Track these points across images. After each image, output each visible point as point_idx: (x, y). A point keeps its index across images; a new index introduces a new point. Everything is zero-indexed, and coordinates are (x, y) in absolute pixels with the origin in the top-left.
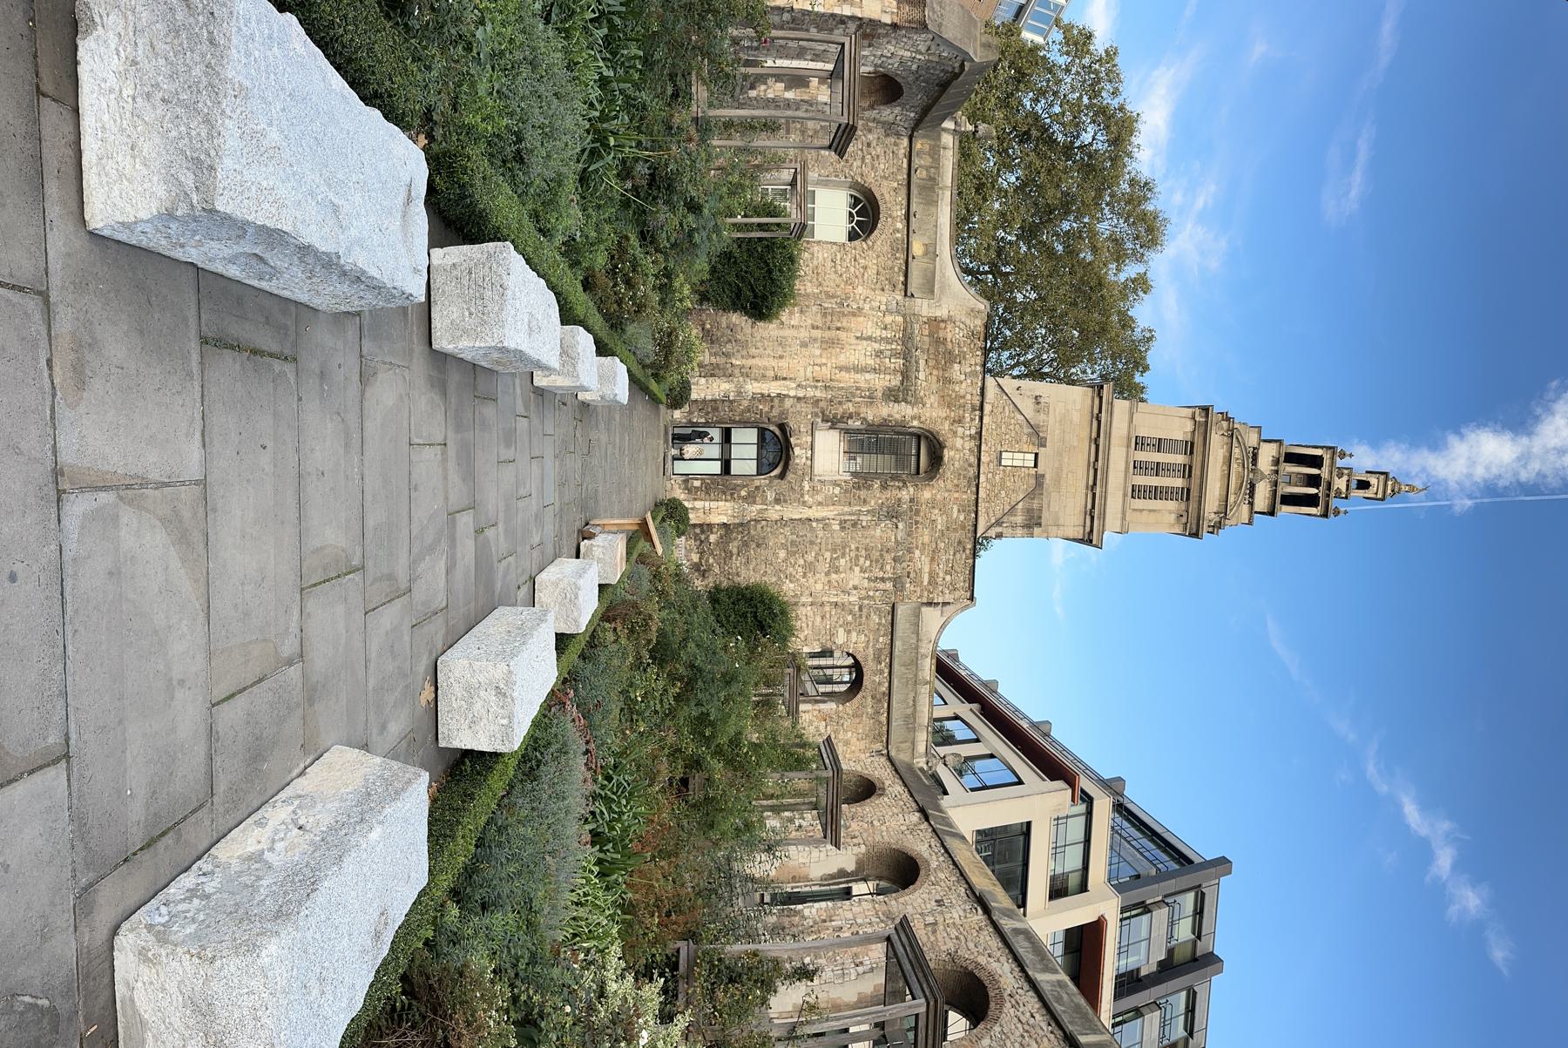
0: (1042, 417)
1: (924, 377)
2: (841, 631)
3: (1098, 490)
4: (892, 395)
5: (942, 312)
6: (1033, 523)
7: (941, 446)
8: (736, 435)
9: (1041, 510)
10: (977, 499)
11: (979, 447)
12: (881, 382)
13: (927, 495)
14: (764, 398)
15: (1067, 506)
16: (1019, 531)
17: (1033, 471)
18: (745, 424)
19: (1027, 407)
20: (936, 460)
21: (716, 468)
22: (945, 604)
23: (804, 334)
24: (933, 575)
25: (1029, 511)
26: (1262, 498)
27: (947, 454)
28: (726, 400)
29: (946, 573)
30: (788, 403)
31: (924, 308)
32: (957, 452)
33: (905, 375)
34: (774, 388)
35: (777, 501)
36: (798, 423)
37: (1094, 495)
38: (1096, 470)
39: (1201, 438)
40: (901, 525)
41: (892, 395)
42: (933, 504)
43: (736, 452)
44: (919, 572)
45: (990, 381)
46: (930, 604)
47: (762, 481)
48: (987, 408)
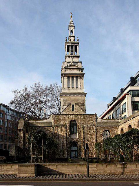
0: (66, 104)
1: (62, 123)
2: (100, 133)
3: (77, 94)
4: (66, 127)
5: (53, 121)
6: (83, 105)
7: (72, 120)
8: (72, 149)
9: (81, 104)
10: (80, 114)
11: (72, 115)
12: (64, 129)
13: (79, 122)
14: (67, 146)
15: (80, 99)
16: (84, 107)
17: (75, 105)
18: (70, 148)
19: (65, 107)
20: (74, 121)
21: (76, 152)
22: (96, 118)
23: (58, 140)
24: (91, 120)
25: (81, 106)
26: (76, 60)
27: (73, 119)
28: (67, 151)
29: (91, 118)
30: (67, 142)
31: (53, 124)
32: (72, 118)
33: (62, 126)
34: (65, 144)
35: (81, 143)
36: (69, 140)
37: (78, 95)
38: (74, 95)
39: (67, 75)
40: (84, 125)
41: (66, 127)
42: (81, 121)
43: (74, 149)
44: (91, 122)
45: (62, 113)
46: (96, 121)
47: (78, 146)
48: (66, 113)
